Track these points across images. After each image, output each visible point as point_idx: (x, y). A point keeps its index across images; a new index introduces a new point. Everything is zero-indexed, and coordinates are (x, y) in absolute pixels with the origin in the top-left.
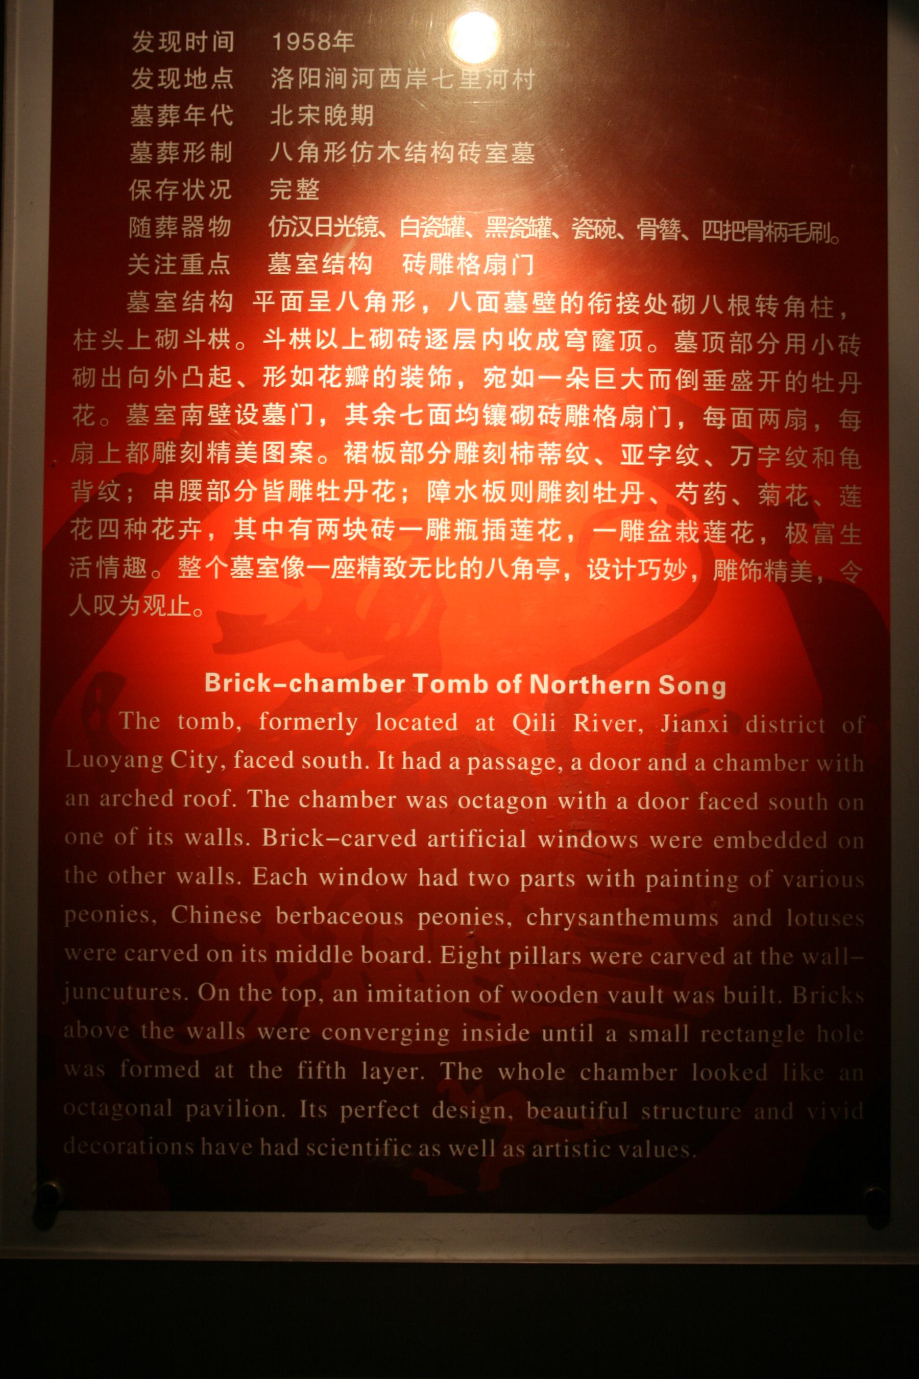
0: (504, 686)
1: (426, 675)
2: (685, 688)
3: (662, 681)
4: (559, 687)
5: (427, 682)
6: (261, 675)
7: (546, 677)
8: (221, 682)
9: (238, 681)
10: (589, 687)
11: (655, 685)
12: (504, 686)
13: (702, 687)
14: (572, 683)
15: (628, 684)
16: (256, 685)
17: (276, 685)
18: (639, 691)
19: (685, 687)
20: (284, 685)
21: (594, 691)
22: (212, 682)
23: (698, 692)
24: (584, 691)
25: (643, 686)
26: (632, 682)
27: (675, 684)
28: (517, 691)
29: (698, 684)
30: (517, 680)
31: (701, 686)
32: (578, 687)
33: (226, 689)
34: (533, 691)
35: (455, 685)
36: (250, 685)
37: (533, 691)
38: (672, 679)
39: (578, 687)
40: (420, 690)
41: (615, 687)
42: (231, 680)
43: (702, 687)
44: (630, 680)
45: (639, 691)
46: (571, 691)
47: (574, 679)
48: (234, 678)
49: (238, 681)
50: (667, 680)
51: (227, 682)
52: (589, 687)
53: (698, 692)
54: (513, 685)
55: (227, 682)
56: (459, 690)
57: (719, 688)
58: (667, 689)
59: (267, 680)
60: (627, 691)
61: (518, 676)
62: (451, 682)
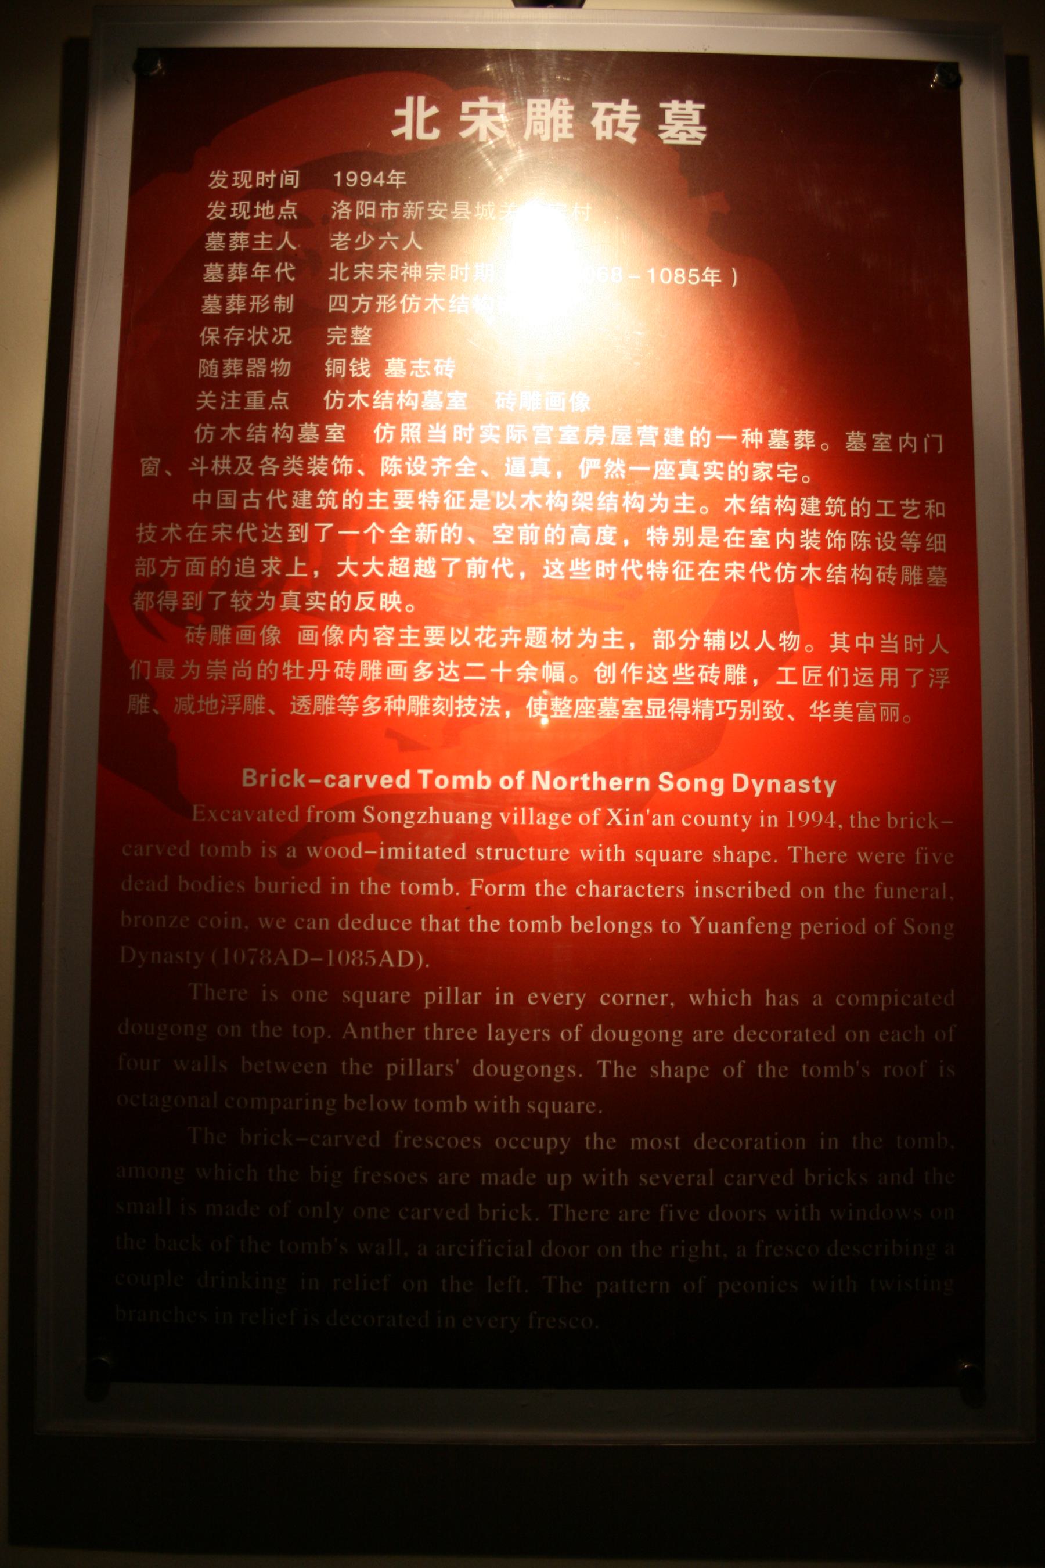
2: (684, 784)
6: (296, 771)
8: (258, 777)
9: (273, 777)
11: (655, 783)
13: (700, 784)
15: (628, 780)
16: (292, 780)
17: (311, 781)
18: (639, 788)
19: (684, 785)
20: (319, 781)
22: (249, 778)
23: (696, 789)
26: (632, 779)
27: (675, 780)
29: (697, 781)
31: (700, 783)
33: (262, 784)
36: (286, 781)
38: (671, 776)
42: (266, 776)
43: (700, 784)
44: (630, 777)
45: (639, 788)
47: (575, 776)
48: (270, 774)
49: (273, 777)
50: (666, 777)
51: (263, 777)
53: (696, 789)
55: (263, 777)
57: (717, 785)
58: (666, 786)
59: (303, 776)
60: (627, 788)
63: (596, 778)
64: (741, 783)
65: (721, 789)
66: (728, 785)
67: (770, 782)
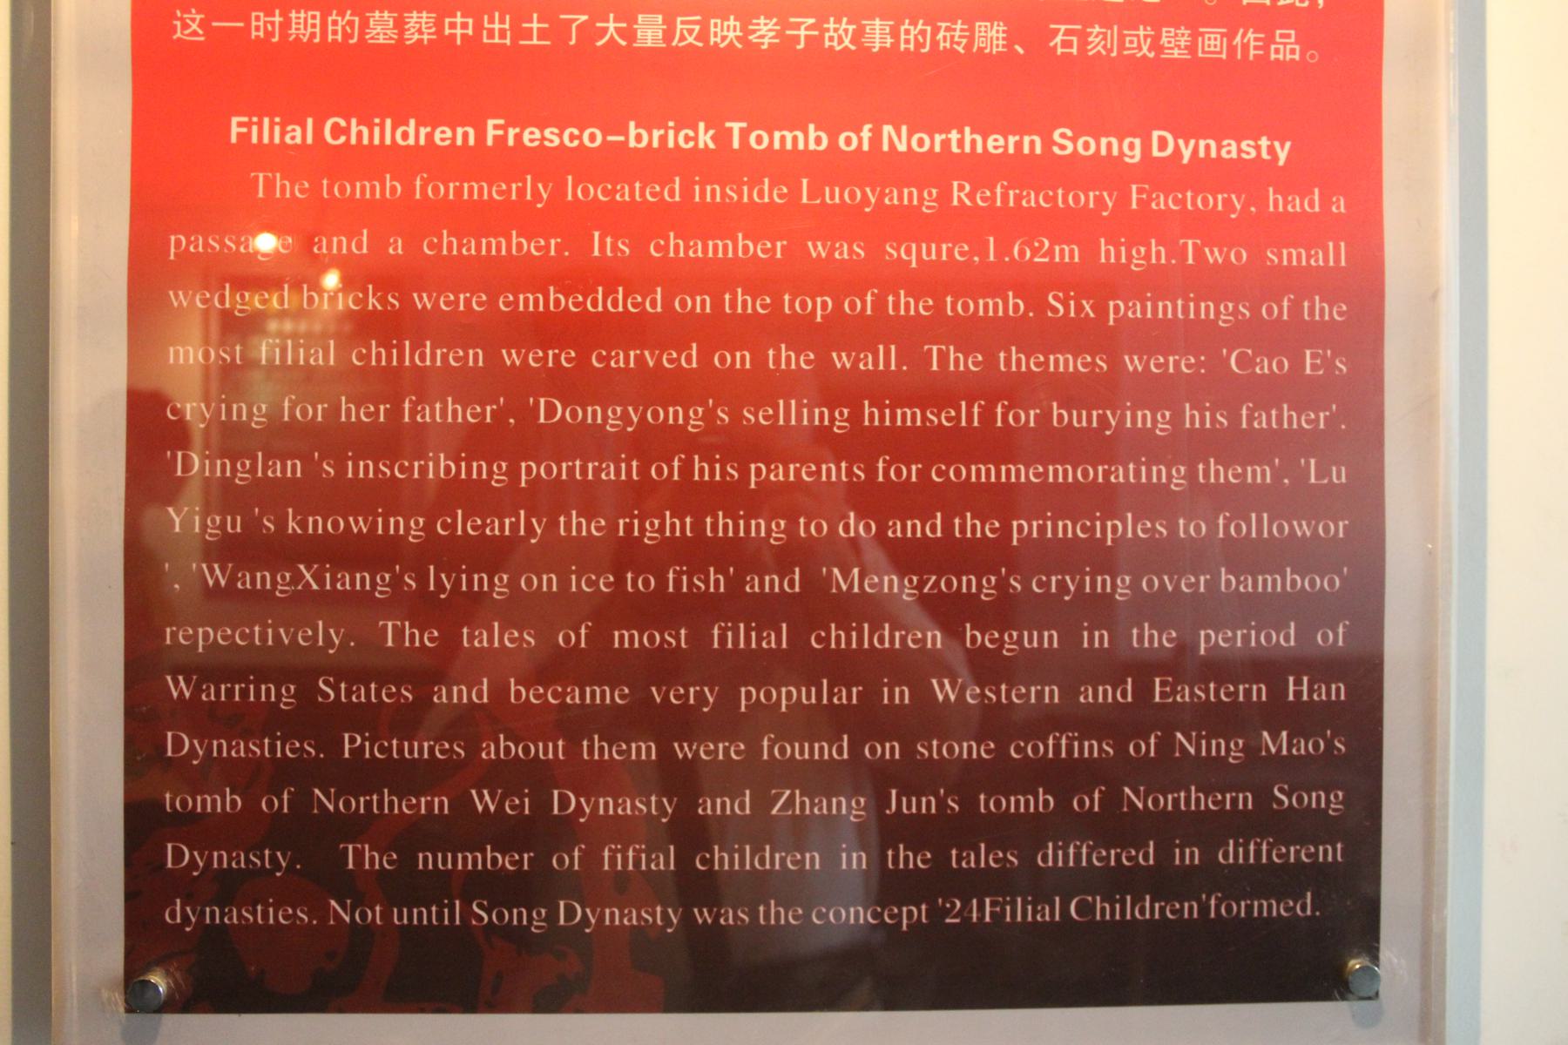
0: (848, 141)
1: (744, 125)
2: (1087, 146)
3: (1056, 136)
4: (921, 143)
5: (744, 134)
7: (904, 129)
10: (961, 143)
11: (1048, 143)
12: (848, 141)
13: (1109, 145)
14: (938, 138)
15: (1012, 140)
18: (1026, 150)
19: (1086, 146)
21: (967, 149)
24: (955, 149)
25: (1032, 143)
28: (866, 147)
29: (1104, 141)
30: (866, 134)
31: (1108, 145)
32: (946, 144)
34: (886, 148)
35: (783, 138)
37: (886, 148)
38: (1069, 133)
39: (946, 144)
40: (736, 145)
41: (995, 143)
43: (1109, 145)
45: (1026, 150)
46: (937, 149)
47: (941, 133)
50: (1063, 136)
52: (961, 143)
53: (1103, 152)
54: (860, 139)
56: (789, 146)
57: (1132, 146)
58: (1063, 147)
60: (1011, 150)
61: (867, 127)
62: (777, 135)
63: (968, 138)
64: (1163, 144)
65: (1138, 152)
66: (1146, 148)
67: (1202, 143)
